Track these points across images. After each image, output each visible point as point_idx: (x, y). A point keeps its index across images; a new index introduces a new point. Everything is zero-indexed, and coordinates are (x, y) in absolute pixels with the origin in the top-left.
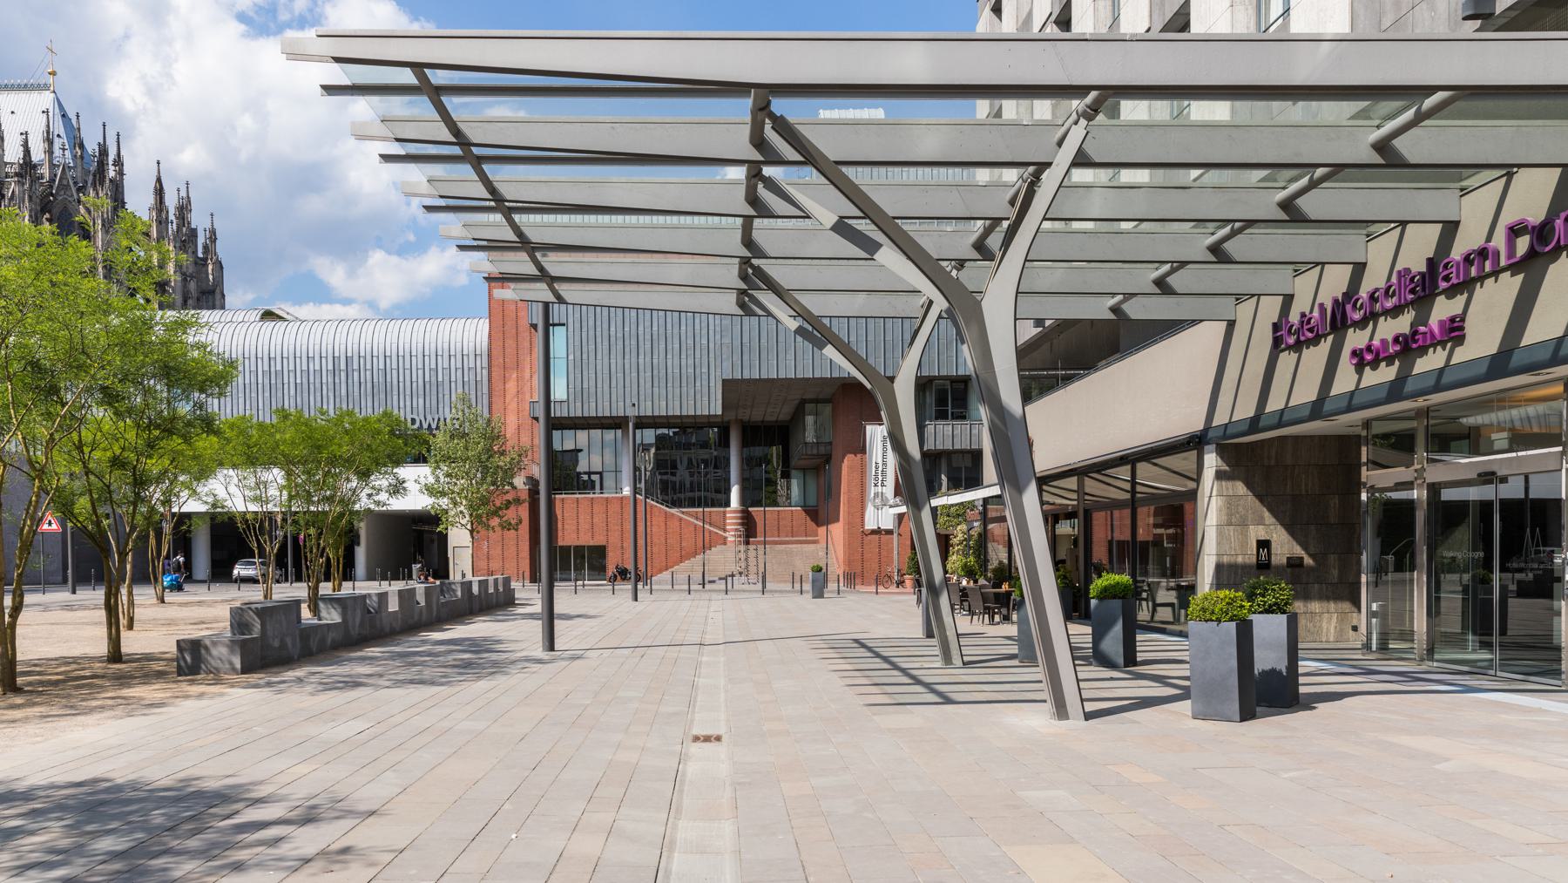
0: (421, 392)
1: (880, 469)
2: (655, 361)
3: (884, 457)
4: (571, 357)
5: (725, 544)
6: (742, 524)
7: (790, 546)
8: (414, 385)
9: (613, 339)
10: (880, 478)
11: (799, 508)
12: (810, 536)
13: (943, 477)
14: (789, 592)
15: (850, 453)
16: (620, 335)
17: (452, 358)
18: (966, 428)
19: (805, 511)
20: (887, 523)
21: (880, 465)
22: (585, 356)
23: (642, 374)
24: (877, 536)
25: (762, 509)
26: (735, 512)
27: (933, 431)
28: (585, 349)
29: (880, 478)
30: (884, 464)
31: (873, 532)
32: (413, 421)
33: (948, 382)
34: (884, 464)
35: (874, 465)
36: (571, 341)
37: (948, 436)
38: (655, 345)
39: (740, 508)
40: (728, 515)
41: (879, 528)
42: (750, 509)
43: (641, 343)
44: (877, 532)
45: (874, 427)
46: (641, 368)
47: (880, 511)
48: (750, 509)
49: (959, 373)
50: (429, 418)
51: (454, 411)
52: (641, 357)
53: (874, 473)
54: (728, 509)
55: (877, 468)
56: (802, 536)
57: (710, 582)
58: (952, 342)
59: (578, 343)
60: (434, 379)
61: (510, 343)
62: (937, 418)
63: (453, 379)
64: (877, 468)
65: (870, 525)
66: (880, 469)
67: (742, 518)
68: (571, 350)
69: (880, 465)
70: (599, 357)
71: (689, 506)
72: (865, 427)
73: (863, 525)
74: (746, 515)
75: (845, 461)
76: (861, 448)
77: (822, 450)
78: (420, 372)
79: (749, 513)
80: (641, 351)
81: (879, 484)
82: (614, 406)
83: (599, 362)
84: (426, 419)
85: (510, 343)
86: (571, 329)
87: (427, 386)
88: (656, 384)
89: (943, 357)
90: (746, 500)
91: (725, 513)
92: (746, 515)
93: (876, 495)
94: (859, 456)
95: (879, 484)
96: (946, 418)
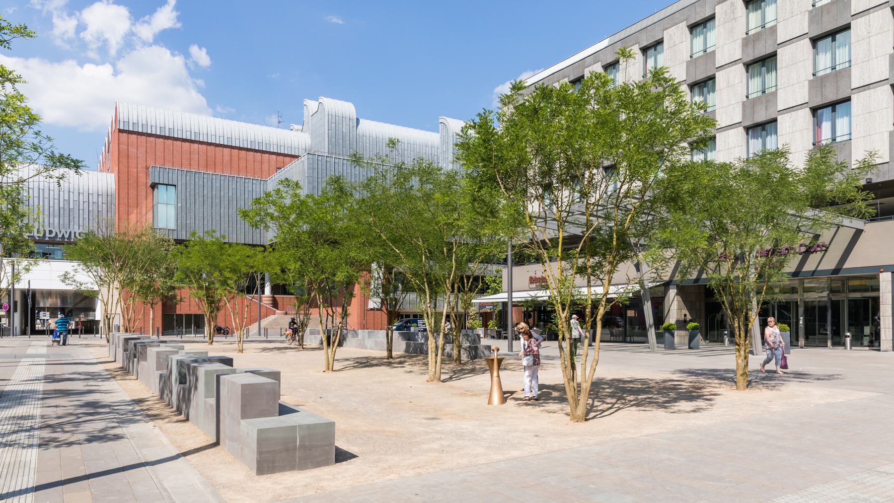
0: (57, 213)
2: (230, 213)
4: (179, 205)
5: (275, 314)
8: (51, 209)
9: (205, 198)
16: (210, 196)
17: (81, 195)
22: (188, 205)
23: (222, 219)
26: (269, 297)
28: (188, 202)
31: (371, 309)
32: (51, 232)
36: (179, 196)
38: (230, 203)
39: (271, 295)
42: (275, 296)
43: (222, 202)
46: (222, 215)
48: (275, 296)
50: (63, 231)
51: (81, 228)
52: (222, 209)
59: (184, 197)
60: (66, 207)
61: (133, 192)
63: (81, 207)
67: (272, 301)
68: (179, 200)
70: (197, 206)
71: (282, 294)
73: (367, 306)
78: (56, 201)
80: (222, 206)
82: (254, 238)
83: (197, 210)
84: (60, 232)
85: (133, 192)
86: (179, 189)
87: (62, 211)
88: (230, 225)
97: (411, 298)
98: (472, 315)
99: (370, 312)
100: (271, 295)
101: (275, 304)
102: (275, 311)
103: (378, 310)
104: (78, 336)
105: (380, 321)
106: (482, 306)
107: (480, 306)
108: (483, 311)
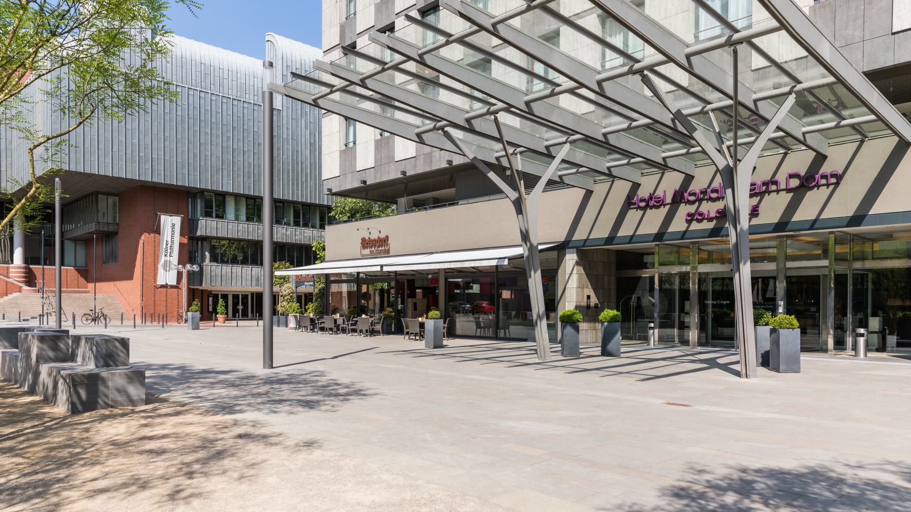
1: (169, 245)
3: (172, 237)
5: (20, 291)
6: (25, 277)
7: (83, 294)
10: (169, 251)
11: (72, 268)
12: (81, 288)
13: (207, 253)
14: (118, 326)
15: (146, 232)
18: (225, 224)
19: (78, 270)
20: (172, 280)
21: (169, 242)
24: (165, 289)
25: (41, 267)
26: (19, 268)
27: (205, 224)
29: (169, 251)
30: (172, 242)
31: (162, 286)
35: (165, 242)
37: (214, 228)
40: (10, 270)
41: (167, 284)
42: (31, 266)
44: (165, 286)
45: (166, 217)
47: (168, 273)
48: (31, 266)
49: (255, 194)
53: (165, 248)
54: (11, 265)
55: (167, 244)
56: (74, 288)
57: (24, 320)
58: (219, 171)
64: (167, 244)
65: (160, 281)
66: (169, 245)
67: (25, 273)
69: (169, 242)
72: (160, 216)
74: (28, 270)
75: (143, 237)
76: (157, 231)
77: (111, 228)
79: (30, 270)
81: (168, 255)
89: (214, 179)
90: (30, 259)
91: (8, 268)
92: (28, 270)
93: (166, 261)
94: (152, 235)
95: (168, 255)
96: (212, 217)
97: (224, 271)
98: (286, 295)
99: (160, 290)
100: (24, 265)
101: (30, 279)
102: (20, 287)
103: (172, 287)
105: (176, 302)
106: (300, 281)
107: (296, 282)
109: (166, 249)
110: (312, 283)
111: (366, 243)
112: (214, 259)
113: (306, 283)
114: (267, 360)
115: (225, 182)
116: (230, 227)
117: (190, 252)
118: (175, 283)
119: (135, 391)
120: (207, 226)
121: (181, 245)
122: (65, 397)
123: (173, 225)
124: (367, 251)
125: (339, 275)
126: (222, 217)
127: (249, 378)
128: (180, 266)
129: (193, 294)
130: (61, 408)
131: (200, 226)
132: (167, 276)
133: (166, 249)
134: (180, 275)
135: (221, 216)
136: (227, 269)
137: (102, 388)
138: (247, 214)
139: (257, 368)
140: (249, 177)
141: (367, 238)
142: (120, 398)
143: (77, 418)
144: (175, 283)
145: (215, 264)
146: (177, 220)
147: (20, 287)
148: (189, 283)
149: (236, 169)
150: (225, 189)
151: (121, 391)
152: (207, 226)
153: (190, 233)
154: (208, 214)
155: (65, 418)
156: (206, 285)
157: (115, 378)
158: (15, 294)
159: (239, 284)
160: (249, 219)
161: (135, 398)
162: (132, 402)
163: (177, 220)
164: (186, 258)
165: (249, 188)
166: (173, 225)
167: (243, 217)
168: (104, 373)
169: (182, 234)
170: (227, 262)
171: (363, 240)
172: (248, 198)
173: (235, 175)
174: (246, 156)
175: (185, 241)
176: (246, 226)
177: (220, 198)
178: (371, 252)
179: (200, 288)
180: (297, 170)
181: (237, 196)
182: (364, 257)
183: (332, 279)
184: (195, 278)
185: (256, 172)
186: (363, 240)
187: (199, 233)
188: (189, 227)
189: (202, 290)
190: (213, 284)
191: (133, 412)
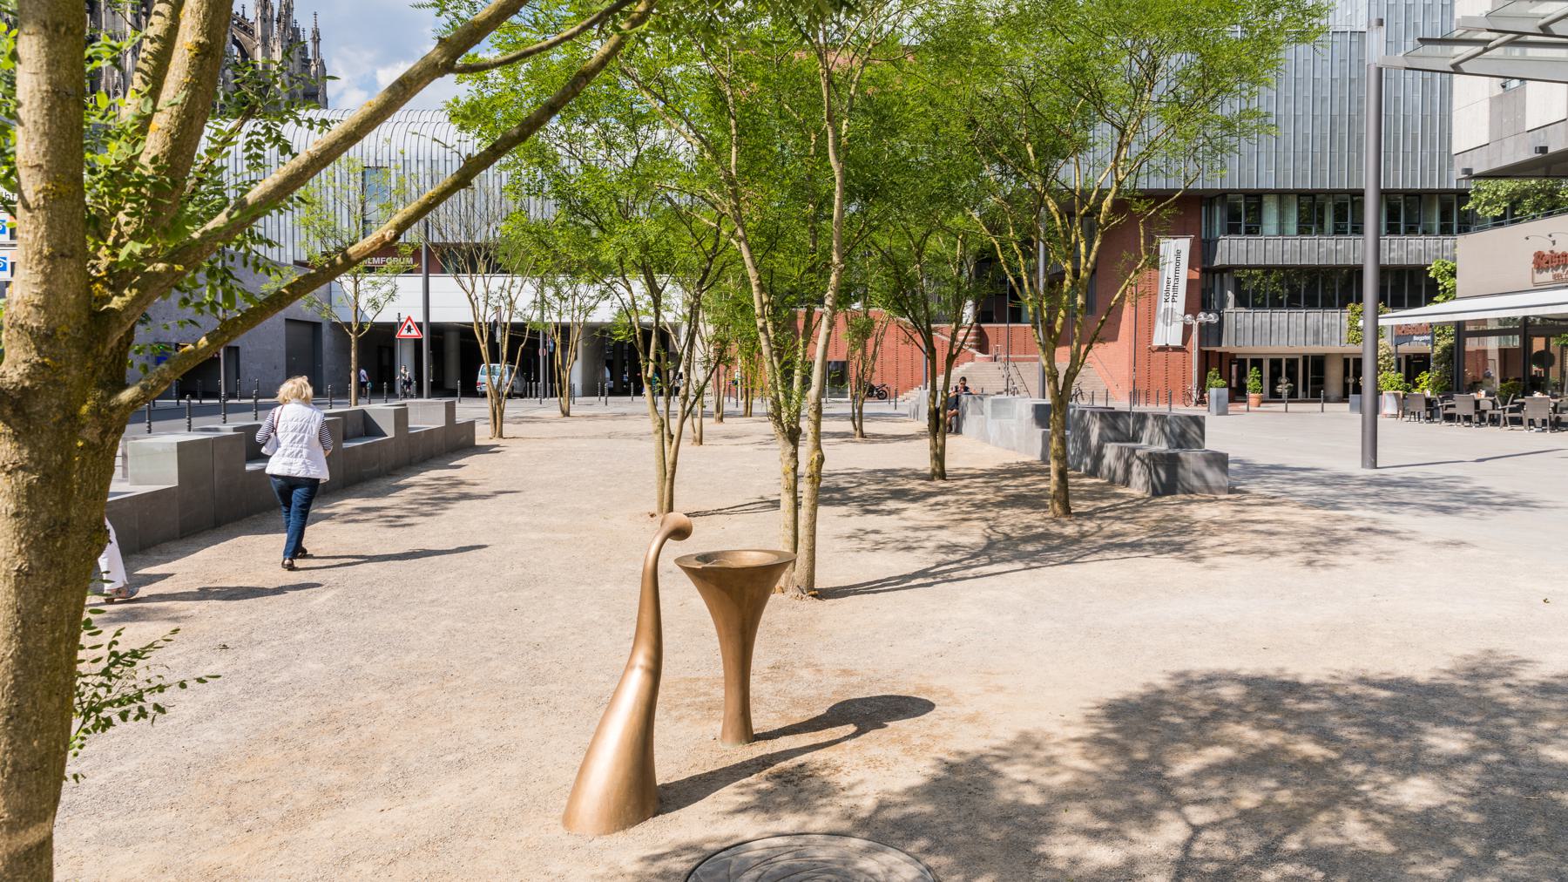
3: (1177, 271)
5: (973, 360)
13: (1230, 295)
21: (1172, 280)
30: (1177, 278)
31: (1161, 349)
33: (1401, 197)
34: (1177, 278)
55: (1168, 283)
58: (1252, 155)
62: (1229, 233)
64: (1168, 283)
65: (1158, 341)
69: (1172, 280)
73: (1150, 342)
76: (1154, 264)
89: (1245, 170)
90: (983, 316)
93: (1166, 310)
96: (1238, 233)
97: (1258, 321)
99: (1156, 354)
102: (973, 355)
103: (1176, 349)
104: (629, 398)
106: (1403, 335)
108: (1405, 348)
109: (1167, 291)
110: (1429, 338)
111: (1542, 262)
112: (1242, 301)
113: (1415, 338)
114: (1368, 455)
115: (1262, 173)
116: (1269, 247)
117: (1203, 291)
118: (1179, 344)
119: (1212, 476)
120: (1233, 250)
121: (1190, 282)
122: (1142, 479)
123: (1179, 252)
124: (1547, 276)
125: (1484, 321)
126: (1257, 233)
127: (1341, 479)
128: (1188, 316)
129: (1206, 360)
130: (1138, 487)
131: (1219, 250)
132: (1168, 333)
133: (1167, 291)
134: (1187, 329)
135: (1254, 230)
136: (1263, 317)
137: (1180, 471)
138: (1299, 222)
139: (1352, 464)
140: (1305, 159)
141: (1547, 252)
142: (1196, 482)
143: (1159, 500)
144: (1179, 344)
145: (1243, 310)
146: (1183, 244)
147: (973, 355)
148: (1200, 345)
149: (1281, 149)
150: (1262, 186)
151: (1200, 476)
152: (1233, 250)
153: (1204, 262)
154: (1233, 230)
155: (1149, 499)
156: (1227, 345)
157: (1192, 459)
158: (968, 365)
159: (1284, 341)
160: (1303, 230)
161: (1213, 484)
162: (1210, 489)
163: (1183, 244)
164: (1197, 302)
165: (1305, 177)
166: (1179, 252)
167: (1292, 225)
168: (1182, 454)
169: (1191, 266)
170: (1262, 306)
171: (1539, 256)
172: (1301, 194)
173: (1281, 160)
174: (1300, 125)
175: (1196, 276)
176: (1298, 243)
177: (1254, 200)
178: (1554, 276)
179: (1218, 349)
180: (1396, 133)
181: (1281, 194)
182: (1539, 288)
183: (1469, 328)
184: (1211, 333)
185: (1318, 149)
186: (1539, 256)
187: (1217, 262)
188: (1203, 253)
189: (1221, 354)
190: (1240, 342)
191: (1217, 500)
